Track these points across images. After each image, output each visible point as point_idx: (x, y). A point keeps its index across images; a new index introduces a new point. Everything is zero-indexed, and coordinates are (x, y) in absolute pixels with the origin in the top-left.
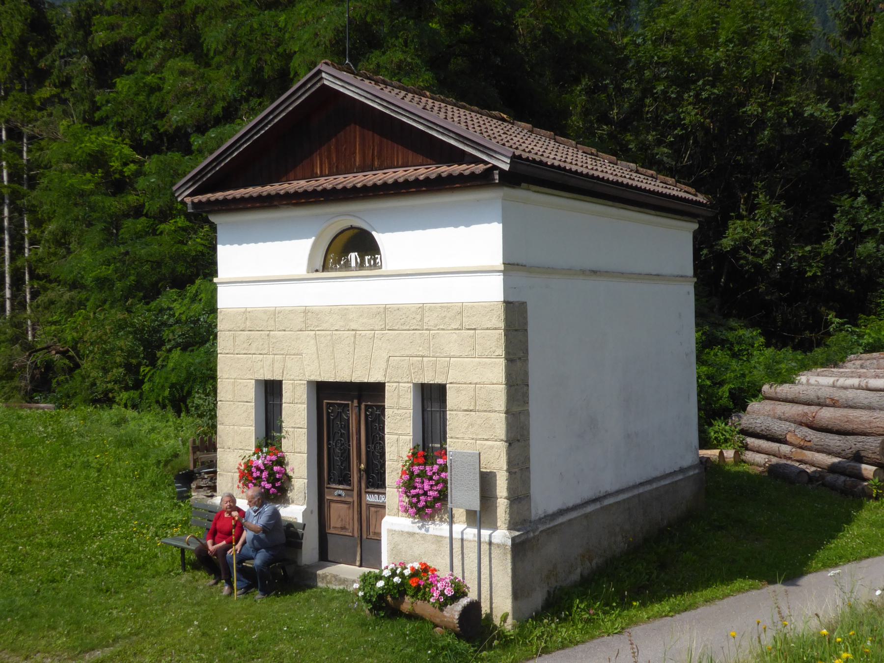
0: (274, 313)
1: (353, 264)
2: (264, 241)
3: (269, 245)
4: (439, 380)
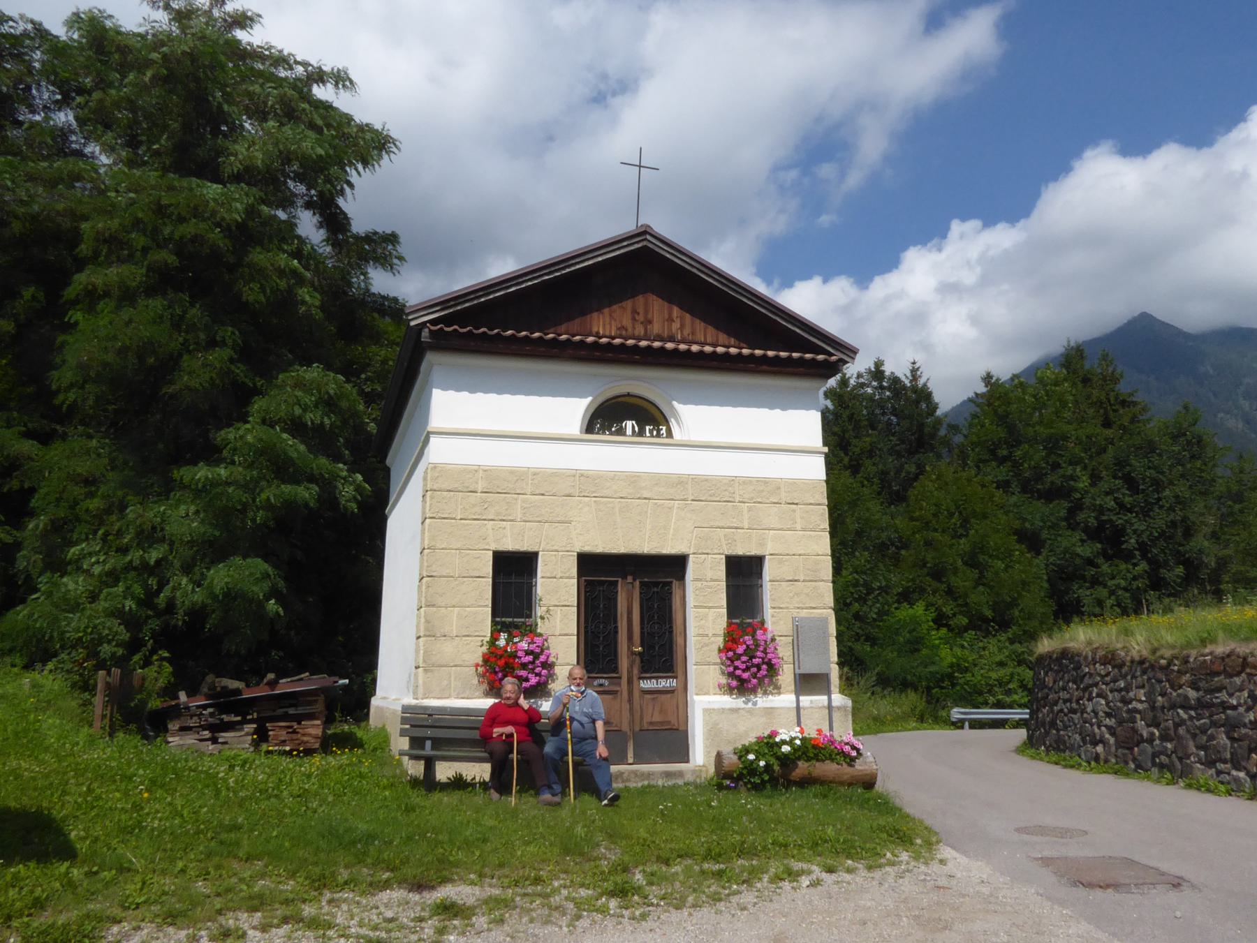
0: (518, 475)
1: (629, 431)
2: (486, 392)
3: (507, 398)
4: (753, 551)
